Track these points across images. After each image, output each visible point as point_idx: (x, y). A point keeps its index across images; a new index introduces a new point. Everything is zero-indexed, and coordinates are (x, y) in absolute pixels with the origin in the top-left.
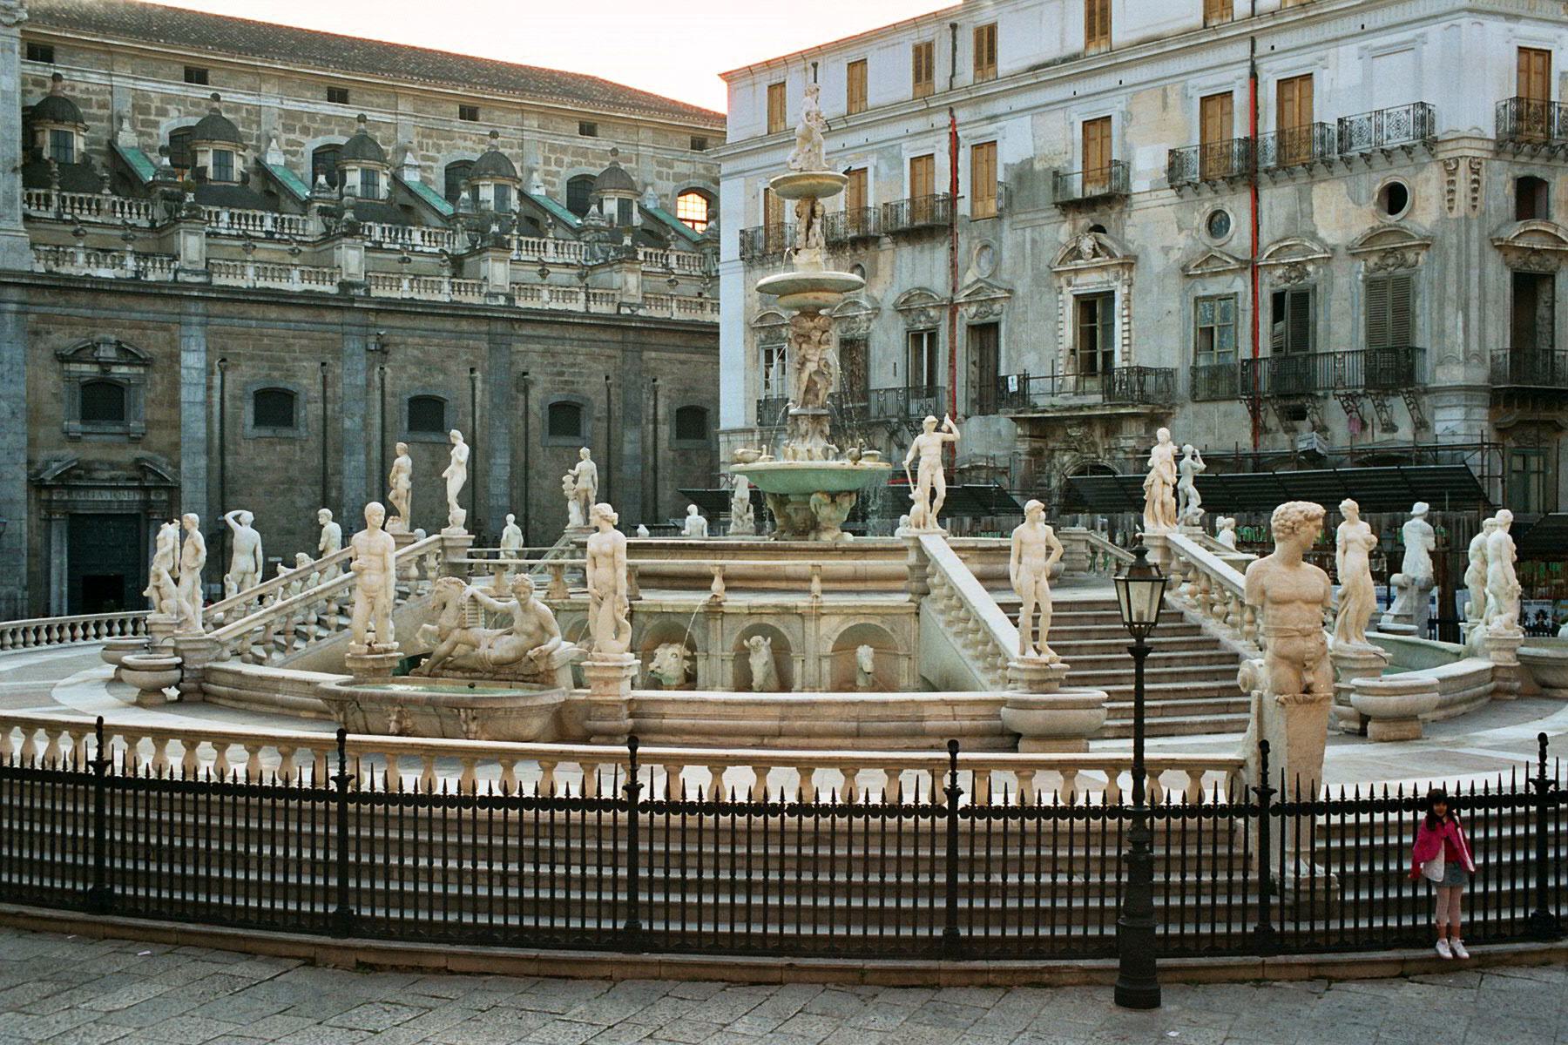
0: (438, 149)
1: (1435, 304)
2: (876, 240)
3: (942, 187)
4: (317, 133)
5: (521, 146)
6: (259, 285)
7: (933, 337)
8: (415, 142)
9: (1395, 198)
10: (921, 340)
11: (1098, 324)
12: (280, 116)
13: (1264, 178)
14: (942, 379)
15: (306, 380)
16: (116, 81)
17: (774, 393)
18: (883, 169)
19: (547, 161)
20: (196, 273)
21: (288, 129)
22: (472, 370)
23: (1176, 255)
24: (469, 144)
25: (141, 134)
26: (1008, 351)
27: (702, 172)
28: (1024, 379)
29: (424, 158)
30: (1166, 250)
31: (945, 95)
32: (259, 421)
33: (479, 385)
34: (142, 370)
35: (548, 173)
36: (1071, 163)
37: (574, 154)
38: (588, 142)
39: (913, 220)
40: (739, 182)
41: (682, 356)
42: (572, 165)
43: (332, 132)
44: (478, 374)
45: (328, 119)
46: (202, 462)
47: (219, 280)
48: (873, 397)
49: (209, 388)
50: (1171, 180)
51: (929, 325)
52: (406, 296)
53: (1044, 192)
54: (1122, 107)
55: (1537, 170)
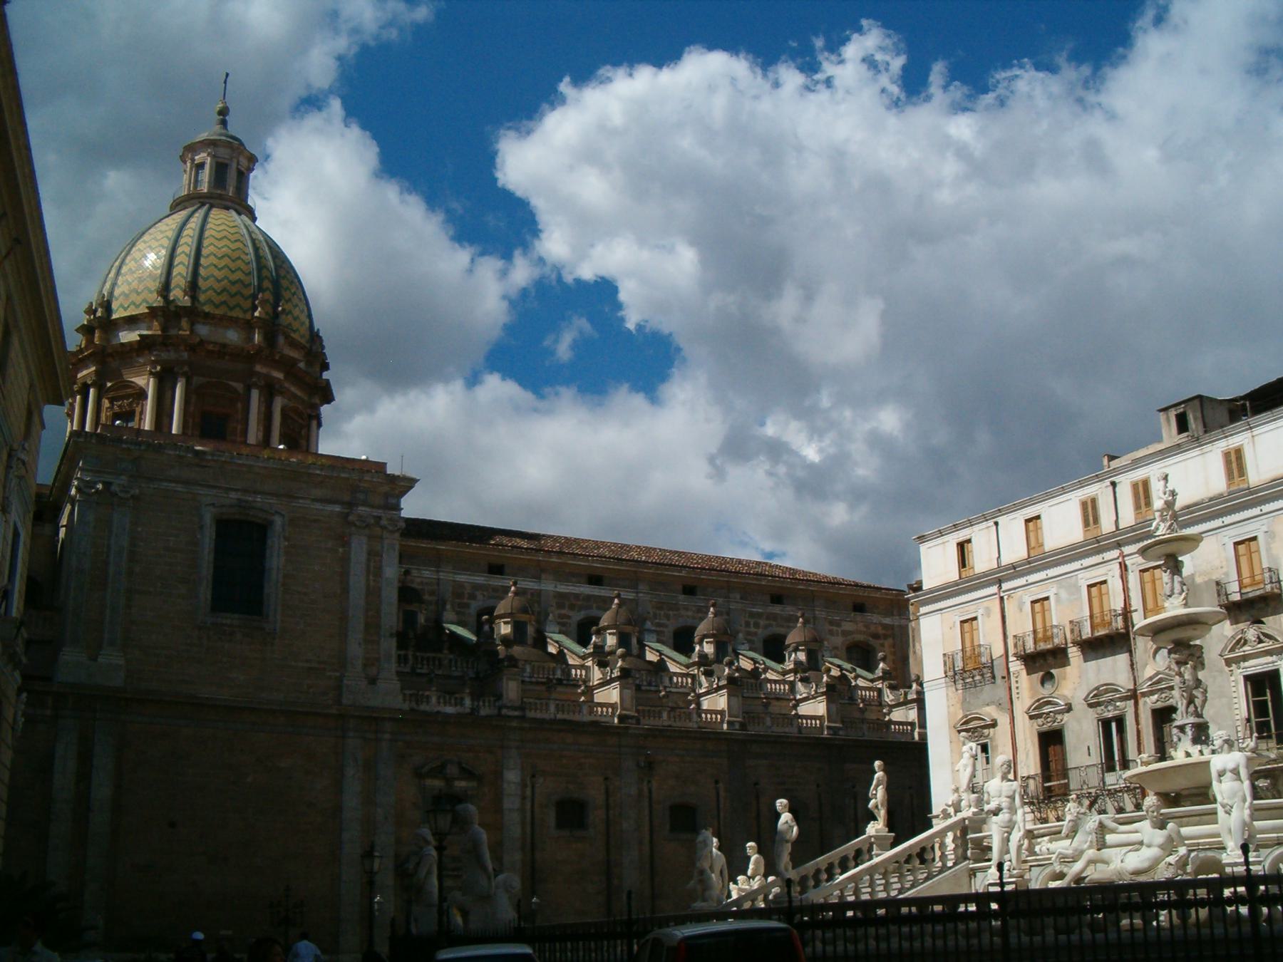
0: (668, 617)
3: (1118, 604)
5: (728, 614)
6: (559, 716)
7: (1120, 721)
10: (1111, 728)
15: (594, 792)
16: (442, 576)
18: (1063, 594)
19: (748, 624)
20: (515, 709)
21: (560, 606)
22: (717, 782)
24: (690, 613)
25: (458, 613)
29: (659, 625)
31: (1113, 535)
32: (560, 825)
33: (722, 793)
34: (474, 784)
35: (749, 633)
36: (1226, 574)
37: (768, 618)
38: (777, 609)
40: (936, 618)
42: (766, 627)
43: (590, 608)
44: (721, 785)
45: (588, 598)
46: (518, 857)
47: (531, 714)
48: (1072, 774)
49: (524, 798)
52: (666, 723)
54: (1265, 528)
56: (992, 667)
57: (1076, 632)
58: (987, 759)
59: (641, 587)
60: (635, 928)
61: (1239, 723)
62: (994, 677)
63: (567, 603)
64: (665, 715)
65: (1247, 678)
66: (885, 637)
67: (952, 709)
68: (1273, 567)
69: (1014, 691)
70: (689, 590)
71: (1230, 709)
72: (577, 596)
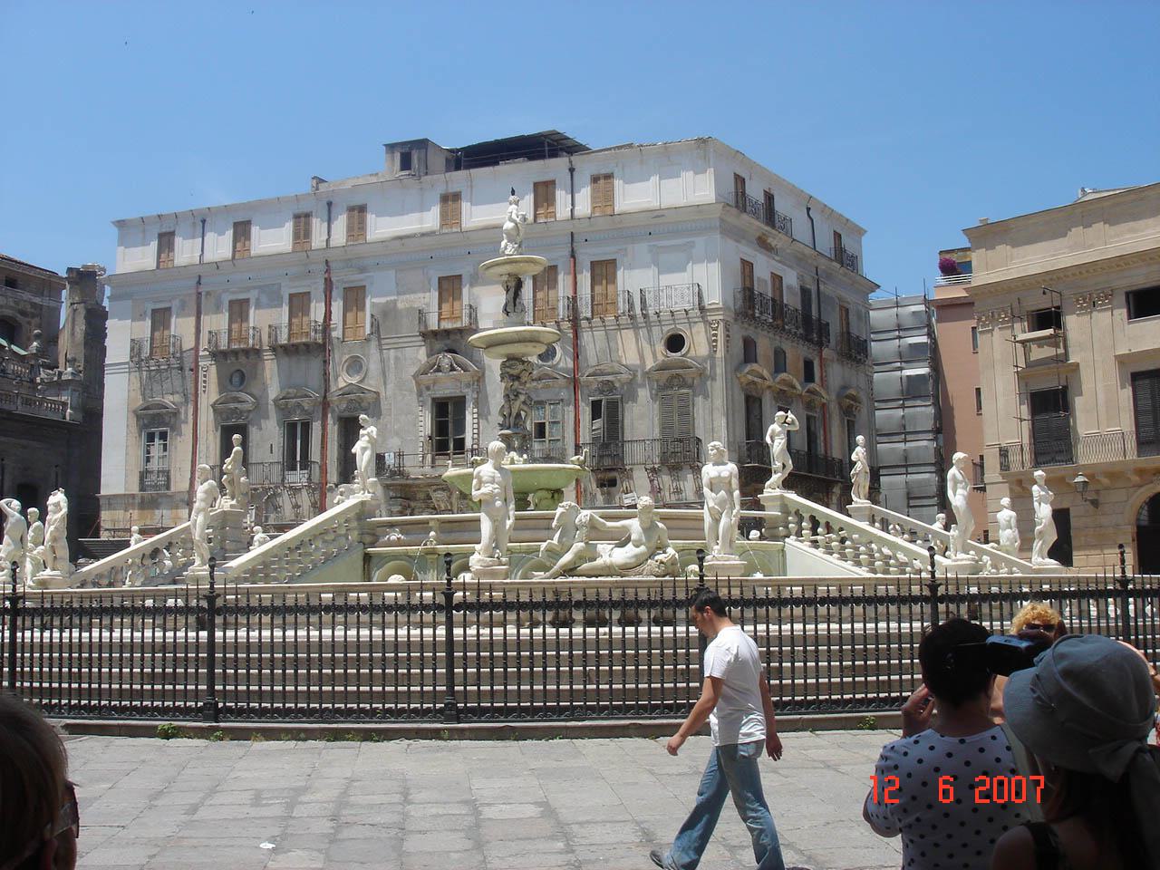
1: (707, 411)
2: (257, 352)
7: (306, 427)
9: (675, 343)
11: (450, 418)
13: (584, 323)
14: (315, 455)
17: (154, 465)
27: (12, 304)
36: (428, 305)
39: (289, 339)
41: (24, 442)
53: (410, 327)
55: (751, 332)
56: (181, 358)
57: (273, 338)
58: (165, 445)
60: (1131, 586)
62: (181, 369)
65: (433, 399)
66: (33, 316)
67: (133, 394)
69: (201, 384)
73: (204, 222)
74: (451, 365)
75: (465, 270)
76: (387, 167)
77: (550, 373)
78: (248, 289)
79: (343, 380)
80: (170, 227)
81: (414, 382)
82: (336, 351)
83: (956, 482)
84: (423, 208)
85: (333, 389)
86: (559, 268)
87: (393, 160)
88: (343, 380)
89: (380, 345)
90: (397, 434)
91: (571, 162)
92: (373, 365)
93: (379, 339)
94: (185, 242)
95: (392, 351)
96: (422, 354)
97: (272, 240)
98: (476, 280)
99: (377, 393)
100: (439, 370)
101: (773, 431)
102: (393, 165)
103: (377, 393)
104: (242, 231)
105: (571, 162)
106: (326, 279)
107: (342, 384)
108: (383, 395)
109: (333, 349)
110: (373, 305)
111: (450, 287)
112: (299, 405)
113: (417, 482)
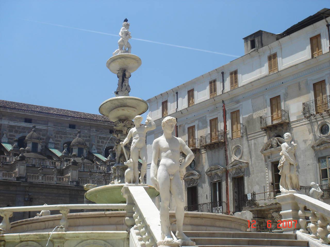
0: (61, 138)
4: (20, 132)
5: (89, 137)
7: (220, 184)
8: (54, 135)
12: (8, 127)
14: (224, 199)
19: (98, 142)
21: (10, 131)
23: (309, 143)
24: (72, 136)
26: (248, 185)
28: (254, 195)
30: (305, 141)
39: (211, 141)
45: (24, 128)
50: (304, 114)
51: (219, 179)
52: (41, 181)
53: (258, 127)
59: (49, 124)
61: (268, 185)
63: (14, 130)
64: (40, 178)
68: (286, 110)
70: (72, 126)
71: (265, 178)
72: (19, 127)
73: (177, 93)
74: (277, 144)
75: (281, 92)
76: (243, 49)
77: (326, 140)
78: (194, 121)
79: (234, 158)
80: (166, 99)
81: (263, 155)
82: (230, 145)
83: (159, 151)
84: (261, 66)
85: (230, 162)
86: (327, 81)
87: (247, 44)
88: (234, 158)
89: (247, 138)
90: (258, 184)
91: (327, 21)
92: (245, 150)
93: (247, 135)
94: (172, 104)
95: (252, 140)
96: (265, 140)
97: (202, 96)
98: (287, 97)
99: (247, 163)
100: (272, 147)
101: (131, 132)
102: (248, 47)
103: (247, 163)
104: (191, 94)
105: (327, 21)
106: (223, 110)
107: (233, 160)
108: (250, 164)
109: (228, 144)
110: (243, 119)
111: (275, 102)
112: (216, 174)
113: (263, 208)
